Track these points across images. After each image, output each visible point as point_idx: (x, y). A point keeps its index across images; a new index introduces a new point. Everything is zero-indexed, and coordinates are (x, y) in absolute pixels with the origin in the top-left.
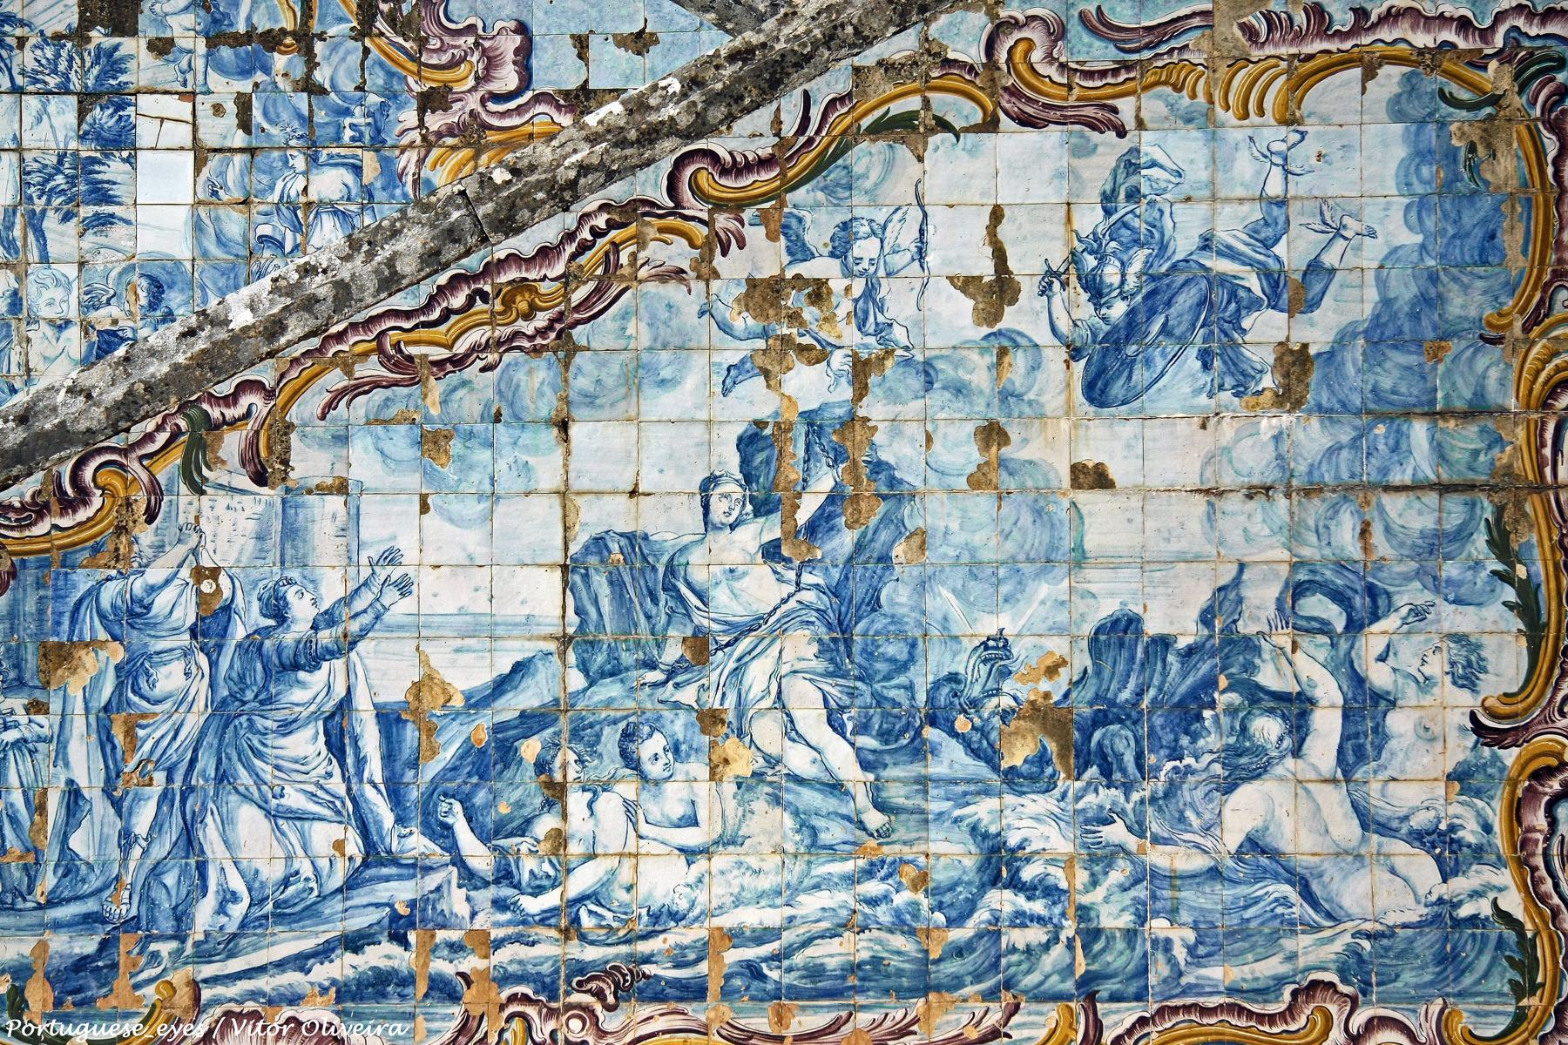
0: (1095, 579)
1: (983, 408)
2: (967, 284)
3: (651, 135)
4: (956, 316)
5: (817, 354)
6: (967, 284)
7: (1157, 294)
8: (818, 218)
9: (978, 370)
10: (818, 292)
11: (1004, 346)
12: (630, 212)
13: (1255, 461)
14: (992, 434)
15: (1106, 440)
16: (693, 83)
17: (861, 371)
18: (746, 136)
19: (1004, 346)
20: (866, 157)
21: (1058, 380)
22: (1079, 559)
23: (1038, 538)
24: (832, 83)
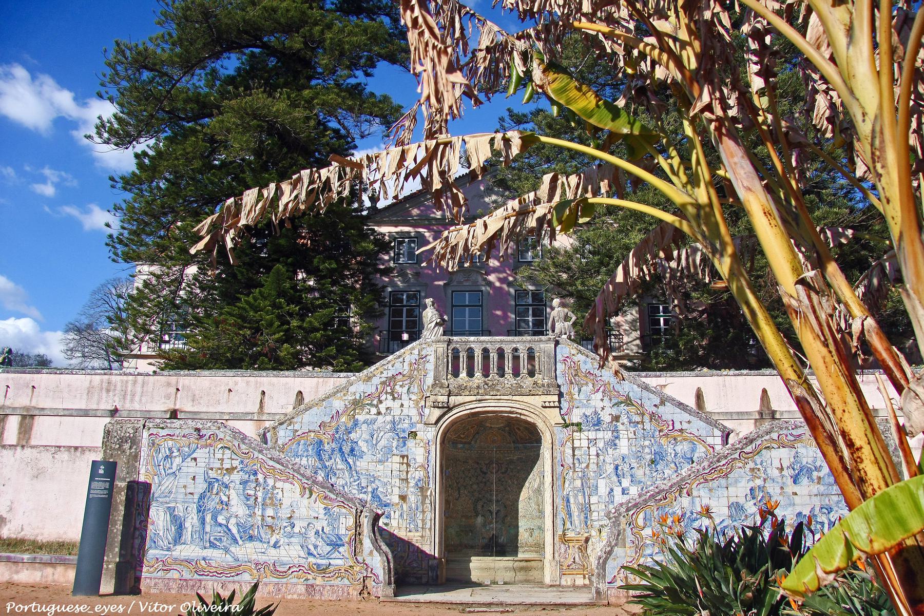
0: (796, 507)
1: (780, 485)
2: (777, 468)
3: (736, 449)
4: (776, 473)
5: (759, 478)
6: (777, 468)
7: (801, 470)
8: (758, 459)
9: (779, 480)
10: (759, 470)
11: (783, 476)
12: (734, 459)
13: (816, 492)
14: (782, 488)
15: (796, 489)
16: (740, 442)
17: (765, 480)
18: (748, 449)
19: (783, 476)
20: (764, 452)
21: (790, 481)
22: (794, 505)
23: (788, 502)
24: (758, 442)
